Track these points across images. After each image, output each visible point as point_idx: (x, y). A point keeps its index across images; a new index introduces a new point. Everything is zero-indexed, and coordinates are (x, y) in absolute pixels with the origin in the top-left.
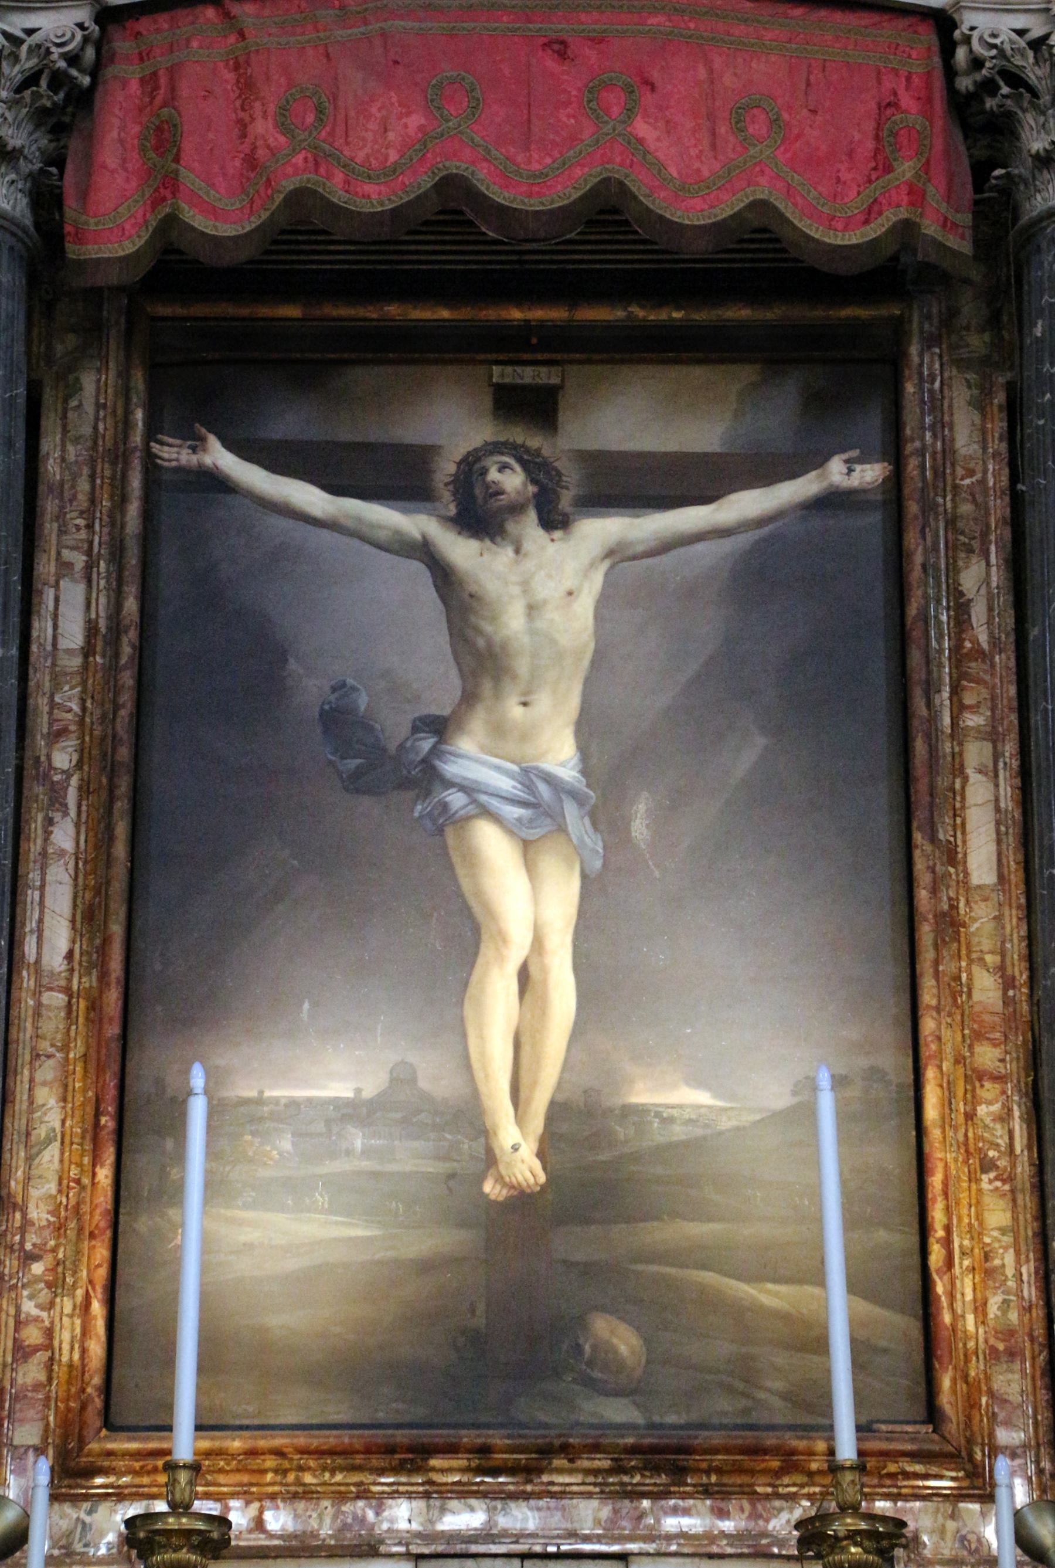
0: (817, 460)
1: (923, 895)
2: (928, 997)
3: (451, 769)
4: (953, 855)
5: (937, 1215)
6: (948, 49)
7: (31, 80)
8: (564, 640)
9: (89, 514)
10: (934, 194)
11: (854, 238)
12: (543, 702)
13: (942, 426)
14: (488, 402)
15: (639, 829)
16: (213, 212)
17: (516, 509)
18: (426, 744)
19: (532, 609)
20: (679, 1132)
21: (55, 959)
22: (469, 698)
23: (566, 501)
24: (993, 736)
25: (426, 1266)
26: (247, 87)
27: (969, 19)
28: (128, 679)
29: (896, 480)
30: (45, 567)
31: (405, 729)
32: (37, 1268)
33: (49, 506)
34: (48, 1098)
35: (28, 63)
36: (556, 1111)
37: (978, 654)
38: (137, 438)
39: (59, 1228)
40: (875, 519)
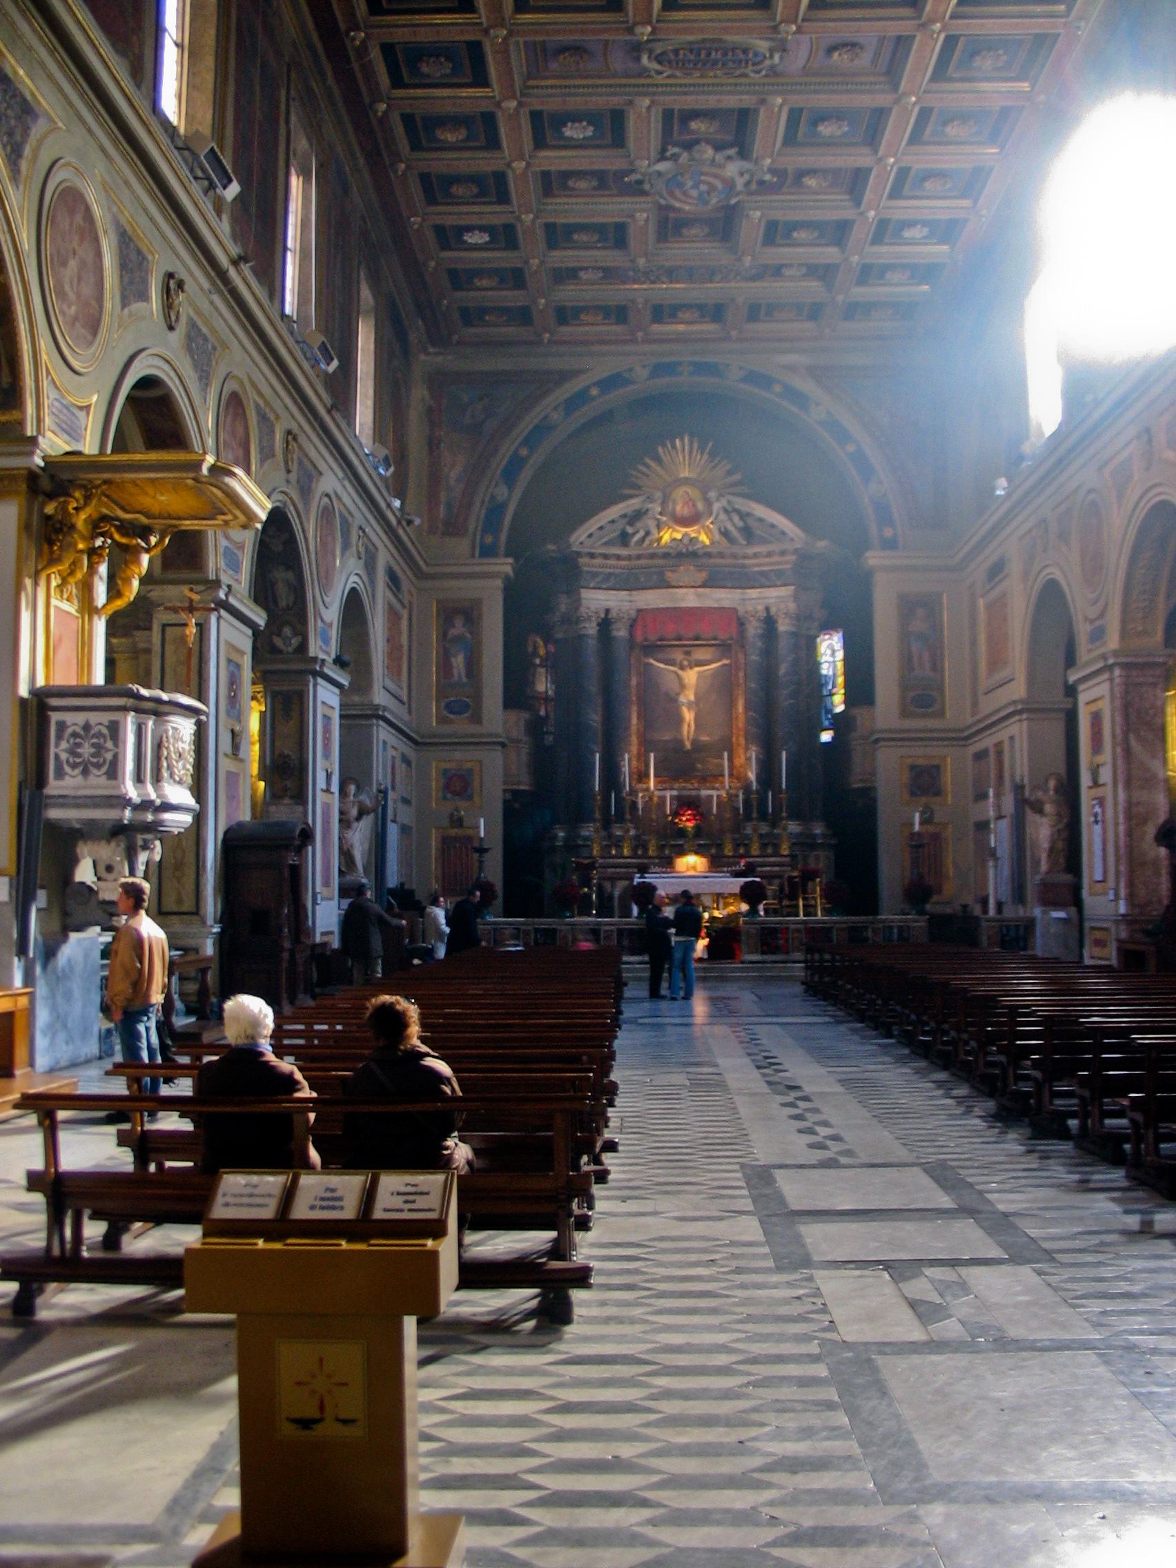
4: (737, 709)
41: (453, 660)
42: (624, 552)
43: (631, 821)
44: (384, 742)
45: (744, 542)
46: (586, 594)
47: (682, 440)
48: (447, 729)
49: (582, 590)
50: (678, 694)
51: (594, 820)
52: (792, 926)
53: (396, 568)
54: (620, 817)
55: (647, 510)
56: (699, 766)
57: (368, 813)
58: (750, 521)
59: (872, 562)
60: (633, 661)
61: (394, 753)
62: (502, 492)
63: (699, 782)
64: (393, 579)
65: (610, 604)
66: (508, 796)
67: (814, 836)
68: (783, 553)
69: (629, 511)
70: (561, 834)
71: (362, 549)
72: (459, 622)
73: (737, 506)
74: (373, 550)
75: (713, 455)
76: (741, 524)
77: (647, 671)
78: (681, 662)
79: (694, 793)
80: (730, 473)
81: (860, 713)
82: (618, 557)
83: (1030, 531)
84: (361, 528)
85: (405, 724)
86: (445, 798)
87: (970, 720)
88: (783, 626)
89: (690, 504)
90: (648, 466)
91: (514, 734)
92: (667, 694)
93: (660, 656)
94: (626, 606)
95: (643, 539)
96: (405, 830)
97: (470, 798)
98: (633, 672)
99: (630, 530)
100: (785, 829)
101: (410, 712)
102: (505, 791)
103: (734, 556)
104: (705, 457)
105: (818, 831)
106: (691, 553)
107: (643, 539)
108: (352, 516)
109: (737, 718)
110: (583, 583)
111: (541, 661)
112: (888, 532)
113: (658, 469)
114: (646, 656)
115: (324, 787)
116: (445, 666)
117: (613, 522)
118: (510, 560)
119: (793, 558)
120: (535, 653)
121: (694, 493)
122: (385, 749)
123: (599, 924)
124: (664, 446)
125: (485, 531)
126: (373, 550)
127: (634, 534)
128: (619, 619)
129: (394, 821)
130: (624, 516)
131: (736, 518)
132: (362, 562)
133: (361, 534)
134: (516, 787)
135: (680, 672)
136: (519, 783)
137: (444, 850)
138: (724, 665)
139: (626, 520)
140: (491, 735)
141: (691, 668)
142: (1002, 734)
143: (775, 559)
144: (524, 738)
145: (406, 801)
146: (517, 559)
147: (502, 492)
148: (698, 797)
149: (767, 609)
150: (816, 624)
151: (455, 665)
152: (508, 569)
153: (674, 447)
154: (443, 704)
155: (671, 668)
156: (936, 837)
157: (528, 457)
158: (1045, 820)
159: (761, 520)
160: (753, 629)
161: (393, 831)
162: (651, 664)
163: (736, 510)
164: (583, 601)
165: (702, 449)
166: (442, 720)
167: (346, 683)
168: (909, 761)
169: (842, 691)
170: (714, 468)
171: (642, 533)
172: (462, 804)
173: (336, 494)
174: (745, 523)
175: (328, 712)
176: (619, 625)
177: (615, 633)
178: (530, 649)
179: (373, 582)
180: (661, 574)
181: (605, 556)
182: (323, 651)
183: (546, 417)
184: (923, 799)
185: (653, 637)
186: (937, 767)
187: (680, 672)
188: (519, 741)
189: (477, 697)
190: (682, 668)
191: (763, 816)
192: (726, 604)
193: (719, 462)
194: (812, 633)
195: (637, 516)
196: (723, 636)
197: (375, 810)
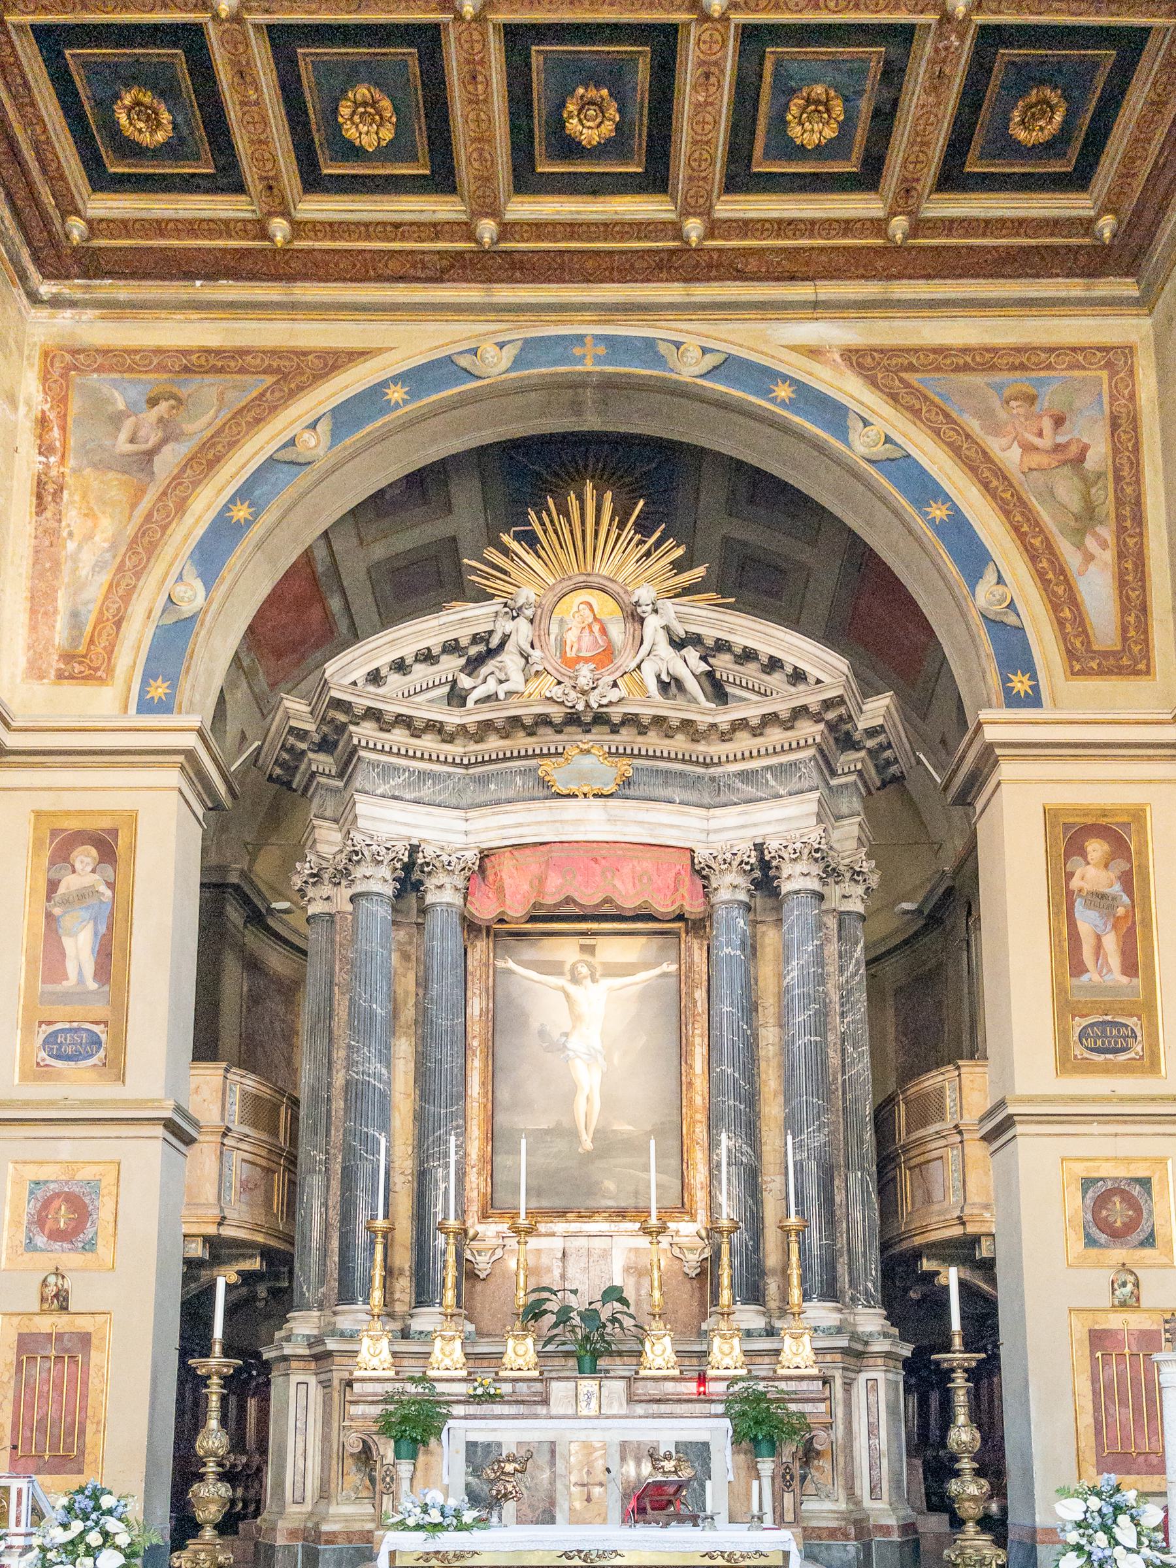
1: (684, 1078)
3: (569, 1045)
6: (693, 858)
7: (463, 869)
11: (670, 910)
13: (691, 955)
14: (578, 949)
17: (585, 977)
18: (564, 1039)
21: (475, 1095)
22: (574, 1027)
23: (597, 976)
24: (702, 1036)
28: (490, 1024)
30: (469, 994)
32: (475, 1170)
34: (475, 1128)
35: (463, 865)
36: (596, 1131)
37: (699, 1015)
38: (491, 961)
39: (479, 1160)
46: (364, 807)
47: (581, 498)
55: (505, 638)
75: (644, 528)
76: (704, 667)
125: (149, 676)
153: (564, 511)
164: (361, 823)
170: (648, 554)
183: (292, 442)
189: (118, 1021)
193: (658, 544)
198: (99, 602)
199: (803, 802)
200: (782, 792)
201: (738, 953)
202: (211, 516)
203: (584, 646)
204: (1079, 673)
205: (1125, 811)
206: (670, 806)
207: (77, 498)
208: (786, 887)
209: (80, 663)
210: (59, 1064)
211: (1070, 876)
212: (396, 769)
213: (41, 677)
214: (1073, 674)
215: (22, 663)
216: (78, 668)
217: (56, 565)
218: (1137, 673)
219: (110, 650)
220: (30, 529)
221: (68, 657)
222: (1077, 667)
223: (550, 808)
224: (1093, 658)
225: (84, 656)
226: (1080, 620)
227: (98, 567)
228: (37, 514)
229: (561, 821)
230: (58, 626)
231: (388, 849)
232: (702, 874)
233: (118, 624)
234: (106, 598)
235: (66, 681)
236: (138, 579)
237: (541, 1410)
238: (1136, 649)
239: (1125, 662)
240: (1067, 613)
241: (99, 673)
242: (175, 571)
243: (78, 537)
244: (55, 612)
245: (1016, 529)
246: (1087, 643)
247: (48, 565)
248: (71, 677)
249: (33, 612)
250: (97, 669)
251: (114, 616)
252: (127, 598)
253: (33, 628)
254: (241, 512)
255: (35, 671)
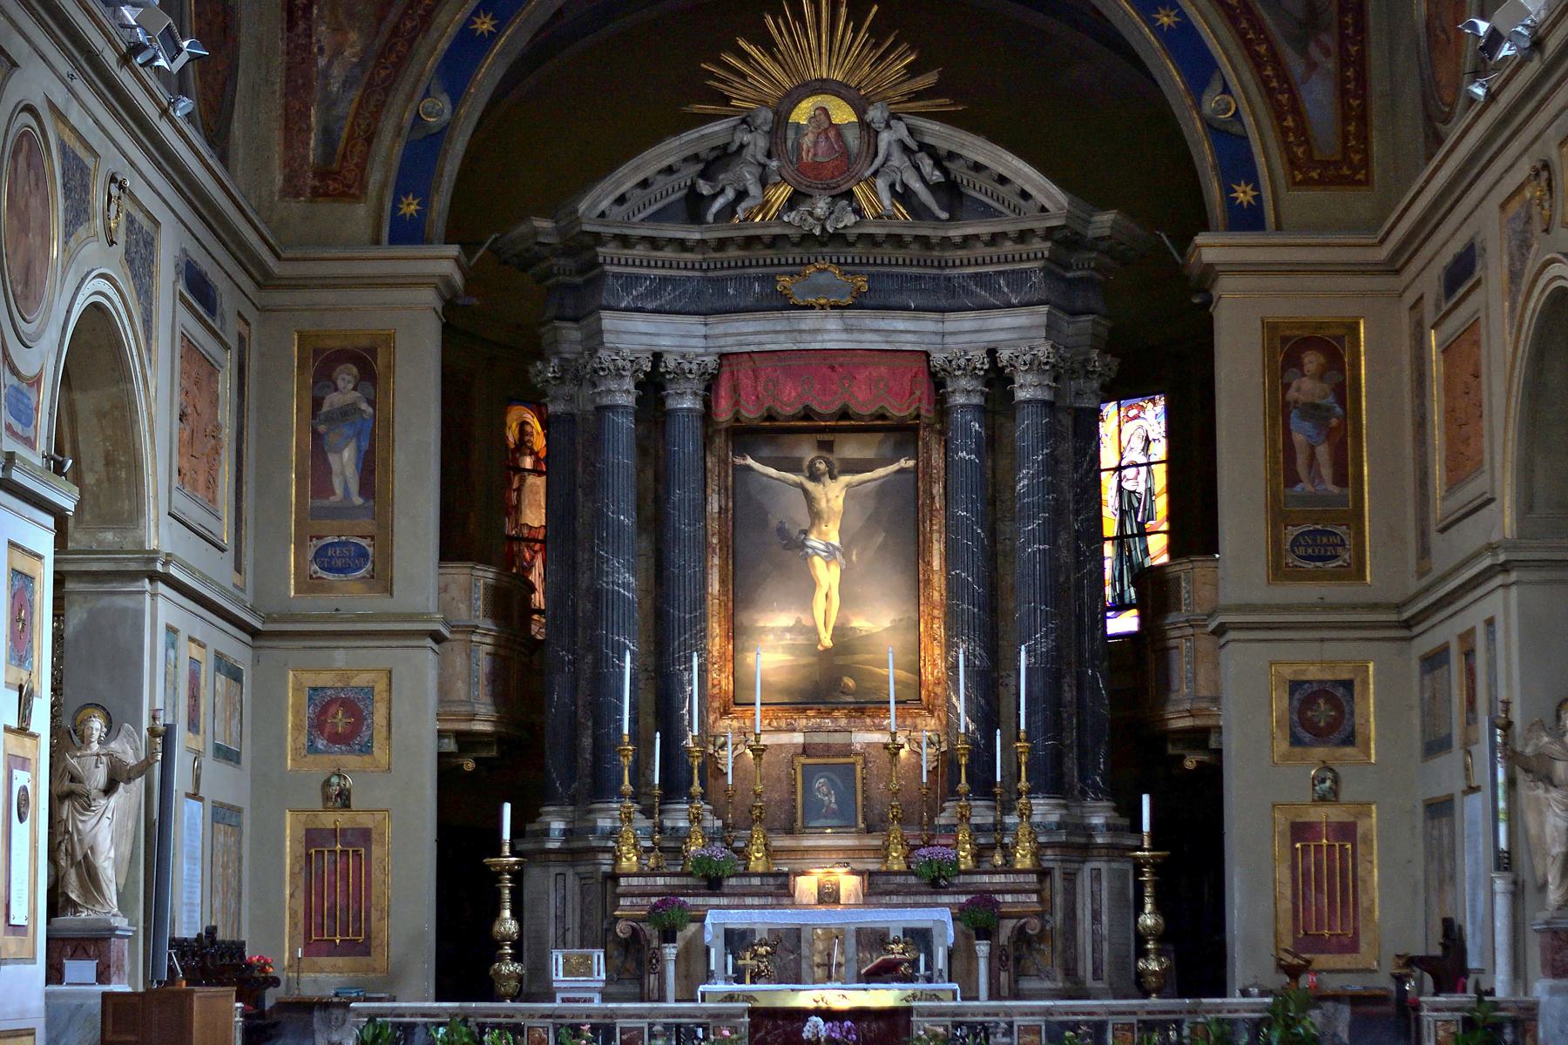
0: (898, 460)
2: (922, 602)
4: (929, 564)
5: (922, 654)
8: (836, 509)
9: (719, 476)
10: (924, 402)
12: (831, 525)
15: (854, 558)
16: (750, 412)
19: (828, 501)
20: (864, 633)
25: (804, 666)
26: (756, 378)
27: (933, 355)
29: (917, 464)
31: (797, 531)
33: (709, 475)
40: (911, 476)
41: (333, 459)
42: (694, 234)
43: (703, 797)
44: (171, 630)
45: (944, 215)
46: (609, 321)
48: (321, 603)
49: (604, 314)
50: (806, 532)
51: (621, 796)
52: (1019, 1021)
53: (205, 264)
54: (674, 787)
55: (742, 146)
56: (850, 683)
57: (129, 780)
58: (957, 169)
59: (1208, 256)
60: (711, 462)
61: (196, 652)
62: (438, 109)
63: (848, 716)
64: (198, 288)
65: (664, 343)
66: (450, 745)
67: (1089, 831)
68: (1023, 236)
69: (703, 149)
70: (557, 825)
71: (119, 225)
72: (346, 376)
73: (928, 140)
74: (147, 225)
75: (878, 33)
76: (937, 176)
77: (739, 487)
78: (812, 462)
79: (838, 739)
80: (913, 71)
81: (1194, 572)
82: (682, 245)
83: (1520, 189)
84: (113, 179)
85: (223, 591)
86: (312, 748)
87: (1414, 585)
88: (1027, 389)
89: (832, 134)
90: (744, 56)
91: (462, 614)
92: (781, 531)
93: (766, 452)
94: (697, 345)
95: (729, 210)
96: (223, 815)
97: (366, 749)
98: (712, 486)
99: (705, 188)
100: (1027, 814)
101: (238, 568)
102: (441, 734)
103: (924, 241)
104: (863, 35)
105: (1097, 820)
106: (833, 236)
107: (729, 210)
108: (96, 155)
109: (928, 582)
110: (605, 298)
111: (537, 461)
112: (1243, 194)
113: (767, 63)
114: (741, 451)
115: (14, 724)
116: (318, 473)
117: (669, 170)
118: (454, 250)
119: (1041, 246)
120: (523, 445)
121: (843, 114)
122: (172, 644)
123: (613, 1014)
124: (777, 13)
125: (400, 194)
126: (147, 225)
127: (714, 197)
128: (681, 373)
129: (195, 796)
130: (695, 158)
131: (927, 164)
132: (120, 248)
133: (115, 191)
134: (463, 726)
135: (810, 485)
136: (472, 717)
137: (308, 856)
138: (902, 471)
139: (701, 166)
140: (410, 618)
141: (833, 477)
142: (1473, 617)
143: (1008, 247)
144: (488, 624)
145: (225, 754)
146: (468, 247)
147: (438, 109)
148: (847, 750)
149: (992, 353)
150: (1096, 385)
151: (335, 467)
152: (448, 268)
154: (310, 554)
155: (791, 477)
156: (1346, 831)
157: (493, 37)
158: (1555, 794)
159: (978, 167)
160: (964, 394)
161: (189, 820)
162: (749, 468)
163: (923, 147)
164: (607, 337)
165: (856, 16)
166: (308, 584)
167: (69, 504)
168: (1288, 672)
169: (1165, 527)
170: (882, 58)
171: (730, 194)
172: (351, 761)
173: (52, 107)
174: (945, 172)
175: (24, 564)
176: (683, 386)
177: (672, 404)
178: (512, 435)
179: (145, 294)
180: (770, 280)
181: (654, 243)
182: (14, 434)
184: (1320, 752)
185: (751, 413)
186: (1348, 685)
187: (810, 485)
188: (473, 630)
189: (384, 535)
190: (815, 477)
191: (983, 786)
192: (908, 343)
193: (894, 46)
194: (1087, 403)
195: (719, 160)
196: (898, 410)
197: (144, 768)
198: (350, 119)
199: (1033, 313)
200: (1014, 301)
201: (973, 457)
202: (452, 31)
203: (820, 152)
204: (1300, 183)
205: (1342, 324)
206: (906, 314)
207: (326, 13)
208: (1022, 395)
209: (335, 180)
210: (324, 575)
211: (1287, 387)
212: (638, 277)
213: (297, 195)
214: (1295, 184)
215: (279, 180)
216: (332, 185)
217: (308, 86)
218: (1359, 183)
219: (362, 167)
220: (282, 46)
221: (322, 174)
222: (1299, 177)
223: (788, 318)
224: (1314, 169)
225: (338, 173)
226: (1302, 129)
227: (347, 84)
228: (290, 29)
229: (801, 331)
230: (312, 143)
231: (632, 361)
232: (938, 382)
233: (369, 141)
234: (357, 114)
235: (320, 199)
236: (387, 95)
237: (786, 901)
238: (1356, 158)
239: (1346, 171)
240: (1289, 122)
241: (352, 191)
242: (422, 88)
243: (328, 52)
244: (309, 129)
245: (1242, 35)
246: (1309, 154)
247: (300, 82)
248: (326, 195)
249: (287, 129)
250: (350, 187)
251: (366, 132)
252: (376, 116)
253: (288, 145)
254: (485, 25)
255: (292, 189)
